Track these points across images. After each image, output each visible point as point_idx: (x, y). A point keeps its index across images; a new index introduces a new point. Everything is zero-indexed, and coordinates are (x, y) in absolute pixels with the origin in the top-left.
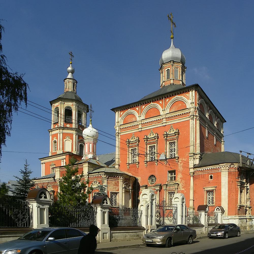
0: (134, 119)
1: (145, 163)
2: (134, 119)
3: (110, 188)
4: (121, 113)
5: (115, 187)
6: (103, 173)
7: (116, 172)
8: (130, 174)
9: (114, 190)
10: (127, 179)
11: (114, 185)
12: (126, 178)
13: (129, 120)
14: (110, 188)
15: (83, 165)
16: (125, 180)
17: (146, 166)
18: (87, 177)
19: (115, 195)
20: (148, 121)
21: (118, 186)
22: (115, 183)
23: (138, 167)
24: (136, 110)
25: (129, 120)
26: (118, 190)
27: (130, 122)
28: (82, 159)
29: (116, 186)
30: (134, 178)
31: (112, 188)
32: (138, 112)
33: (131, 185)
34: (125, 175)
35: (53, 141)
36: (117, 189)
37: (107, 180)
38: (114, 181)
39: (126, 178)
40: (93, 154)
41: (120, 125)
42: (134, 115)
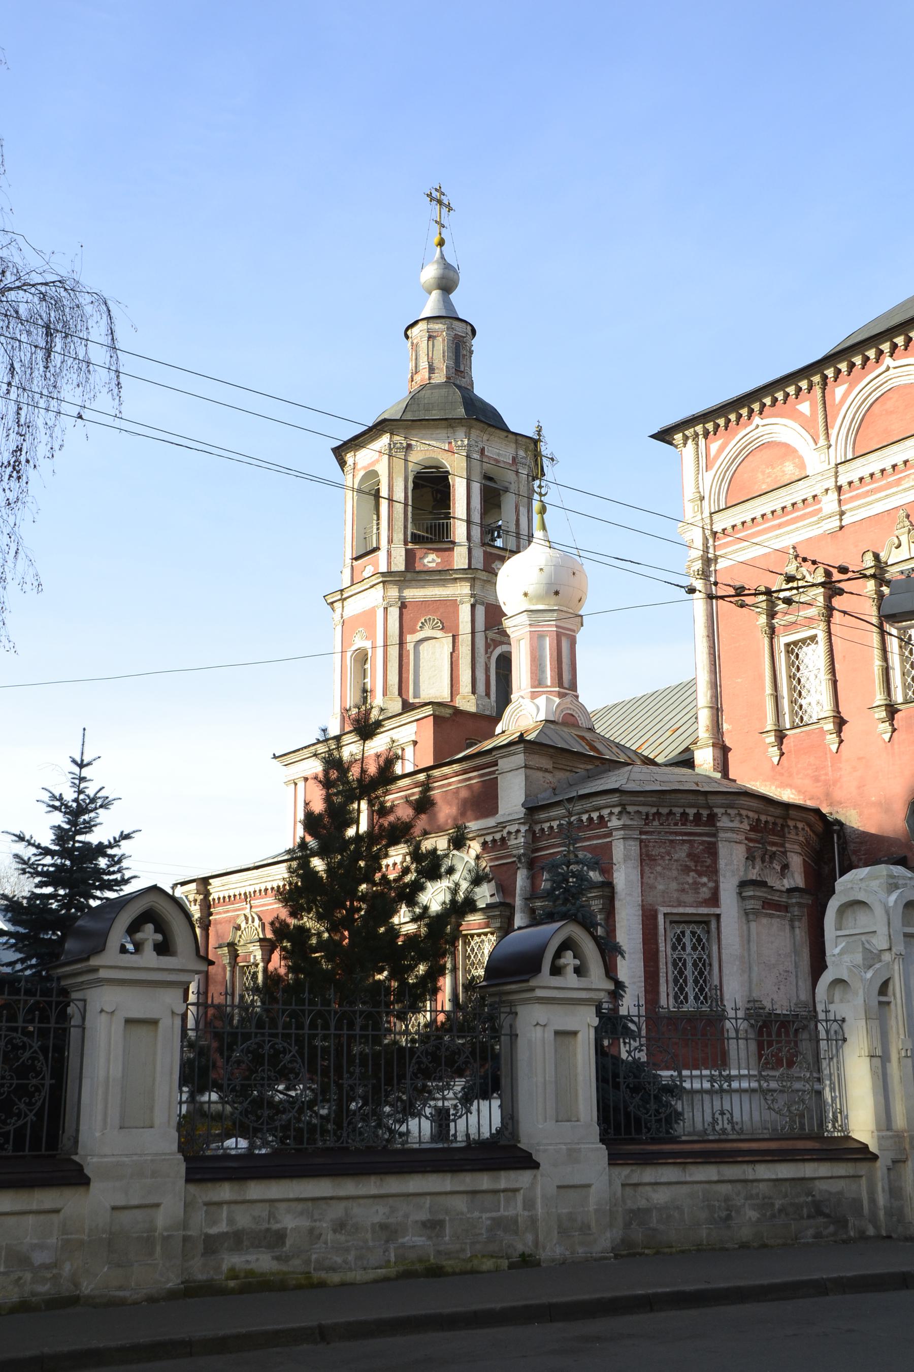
0: (791, 467)
1: (877, 716)
2: (790, 470)
3: (661, 887)
4: (714, 447)
5: (695, 883)
6: (615, 799)
7: (695, 788)
8: (787, 795)
9: (689, 898)
10: (766, 822)
11: (686, 870)
12: (763, 818)
13: (760, 476)
14: (661, 887)
15: (500, 762)
16: (752, 835)
17: (887, 737)
18: (523, 829)
19: (693, 933)
20: (874, 463)
21: (713, 871)
22: (689, 855)
23: (834, 747)
24: (796, 416)
25: (760, 476)
26: (714, 900)
27: (765, 488)
28: (498, 730)
29: (700, 874)
30: (812, 818)
31: (674, 885)
32: (807, 424)
33: (796, 861)
34: (754, 804)
35: (349, 654)
36: (705, 893)
37: (641, 841)
38: (686, 847)
39: (763, 818)
40: (561, 695)
41: (711, 514)
42: (787, 451)
